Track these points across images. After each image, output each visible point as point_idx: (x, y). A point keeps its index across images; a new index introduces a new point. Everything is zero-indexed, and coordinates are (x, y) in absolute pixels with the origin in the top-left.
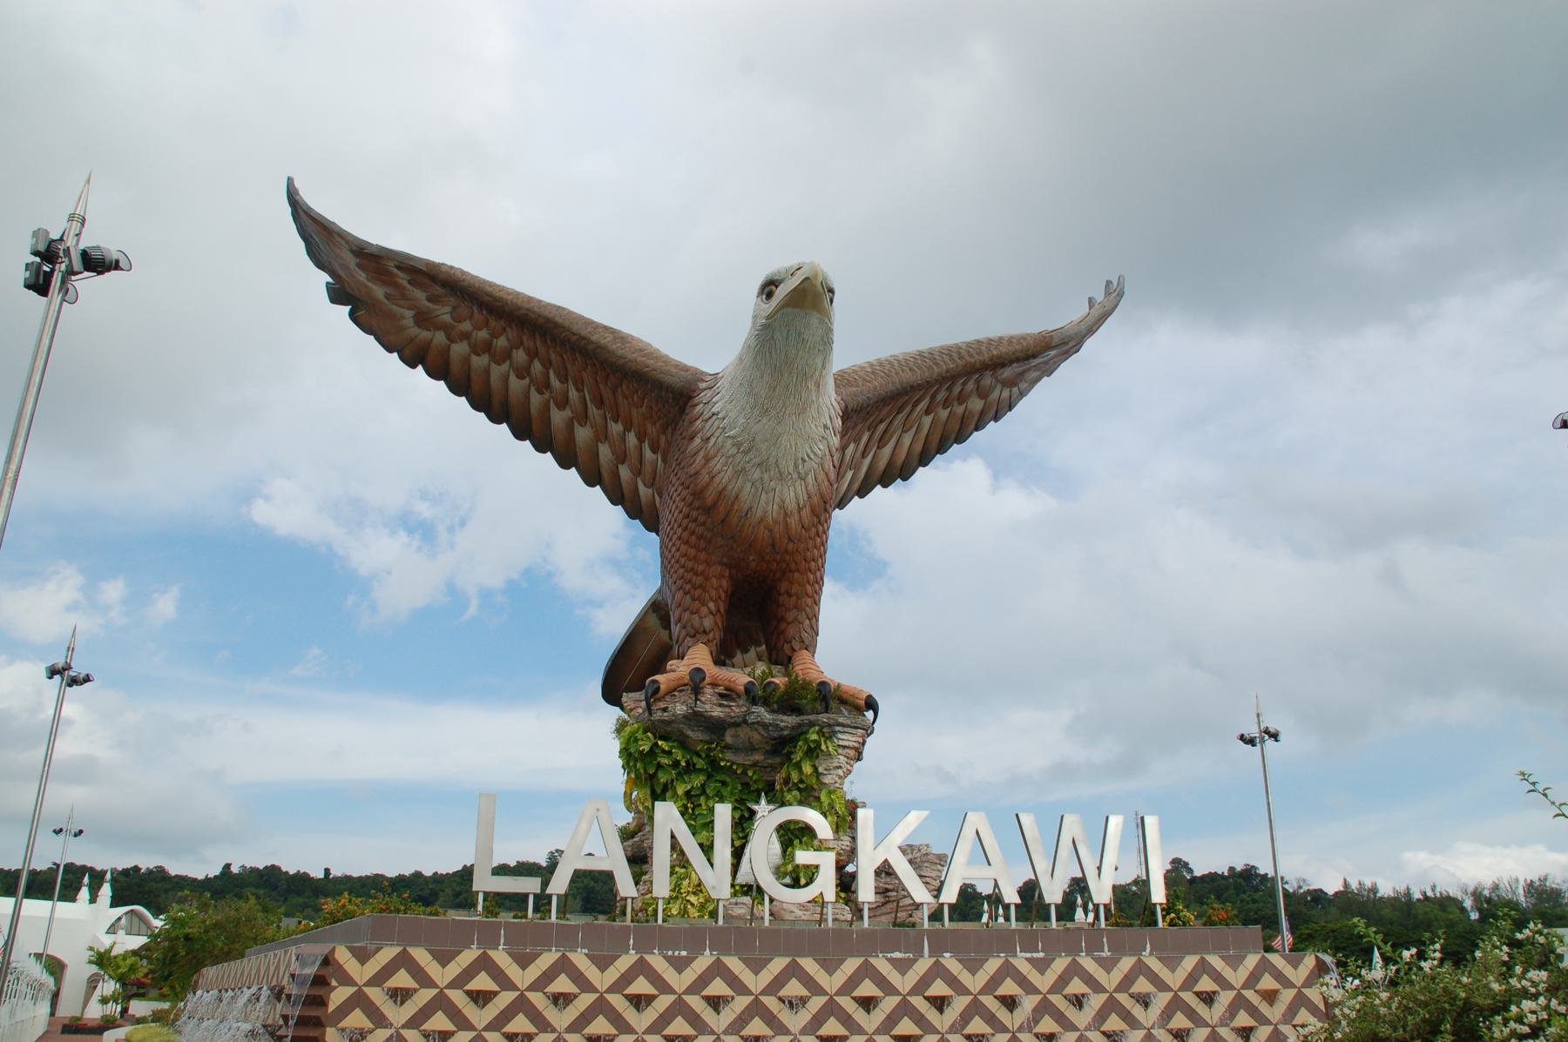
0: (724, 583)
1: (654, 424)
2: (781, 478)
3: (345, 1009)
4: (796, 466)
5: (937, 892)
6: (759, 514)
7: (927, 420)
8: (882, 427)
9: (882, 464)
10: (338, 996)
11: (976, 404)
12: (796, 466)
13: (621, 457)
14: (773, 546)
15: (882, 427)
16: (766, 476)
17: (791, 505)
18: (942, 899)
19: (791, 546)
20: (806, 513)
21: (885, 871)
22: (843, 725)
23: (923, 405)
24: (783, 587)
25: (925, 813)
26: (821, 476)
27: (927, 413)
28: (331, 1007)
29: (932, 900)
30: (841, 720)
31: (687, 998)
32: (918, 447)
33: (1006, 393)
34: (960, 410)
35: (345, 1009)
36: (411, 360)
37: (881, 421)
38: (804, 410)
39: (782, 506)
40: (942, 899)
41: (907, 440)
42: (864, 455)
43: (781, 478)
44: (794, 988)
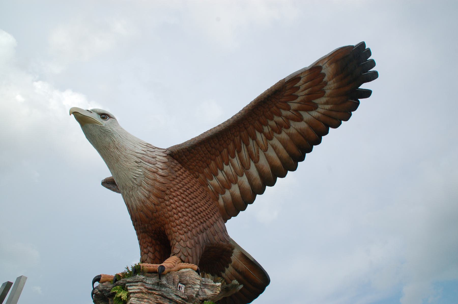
0: (149, 239)
2: (132, 189)
4: (133, 182)
6: (135, 206)
7: (275, 141)
8: (244, 153)
9: (267, 168)
11: (302, 125)
12: (133, 182)
14: (147, 217)
15: (244, 153)
16: (128, 192)
17: (143, 198)
19: (155, 214)
20: (153, 198)
22: (129, 282)
23: (259, 136)
24: (168, 232)
26: (150, 182)
27: (269, 138)
30: (128, 280)
32: (285, 154)
33: (315, 114)
34: (292, 130)
37: (239, 151)
38: (118, 161)
39: (139, 201)
41: (272, 153)
42: (245, 167)
43: (132, 189)
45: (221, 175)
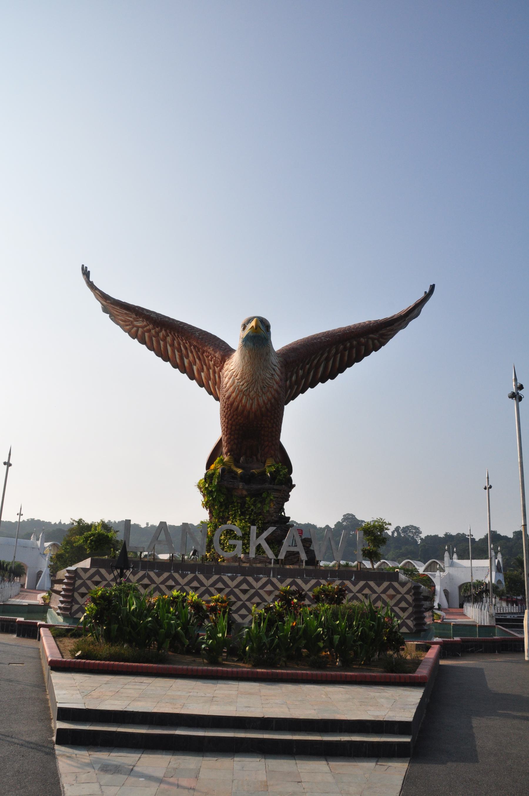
1: (217, 367)
3: (80, 586)
5: (277, 556)
8: (315, 362)
10: (79, 582)
13: (208, 378)
15: (315, 362)
18: (279, 557)
20: (269, 406)
21: (259, 547)
25: (275, 528)
26: (273, 393)
28: (76, 586)
29: (275, 558)
31: (210, 588)
35: (80, 586)
36: (134, 336)
37: (314, 360)
40: (279, 557)
44: (244, 586)
45: (294, 378)
